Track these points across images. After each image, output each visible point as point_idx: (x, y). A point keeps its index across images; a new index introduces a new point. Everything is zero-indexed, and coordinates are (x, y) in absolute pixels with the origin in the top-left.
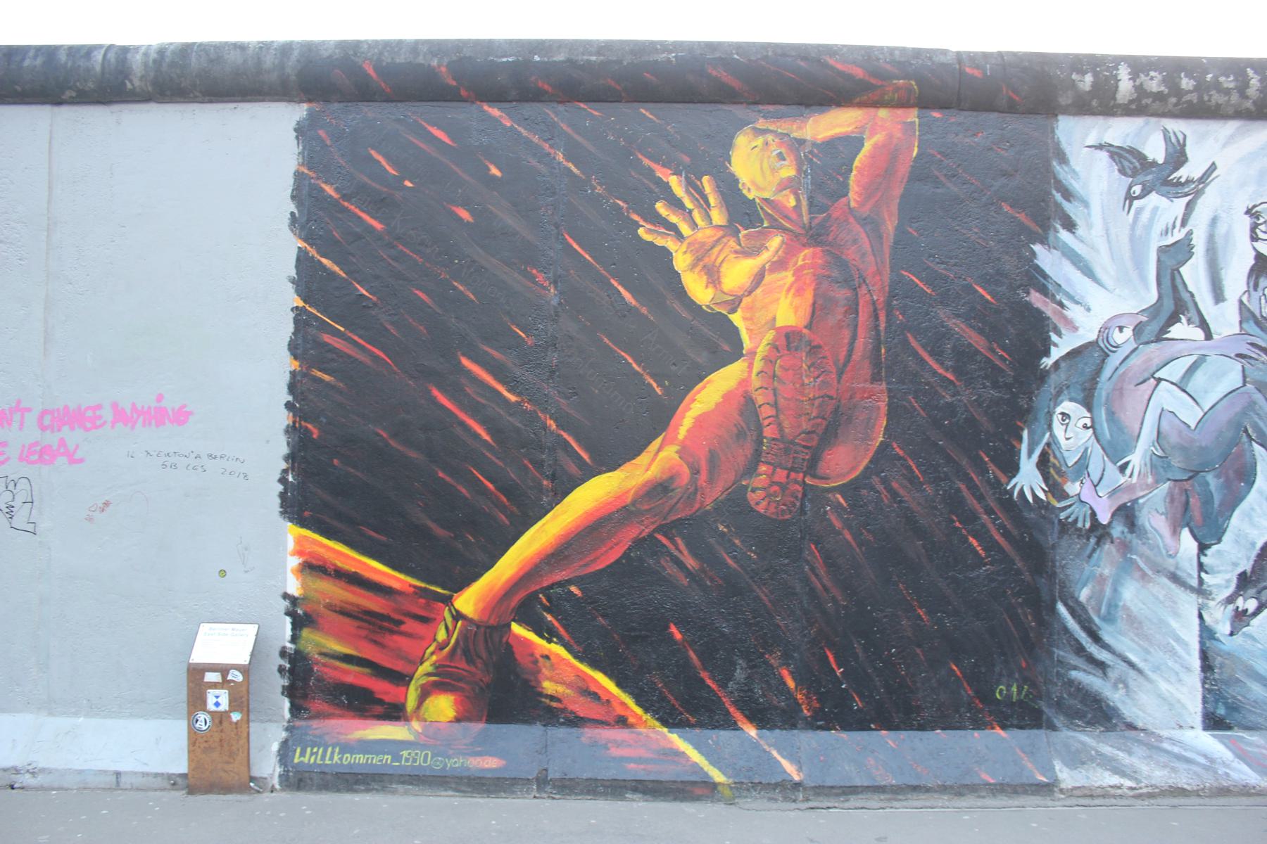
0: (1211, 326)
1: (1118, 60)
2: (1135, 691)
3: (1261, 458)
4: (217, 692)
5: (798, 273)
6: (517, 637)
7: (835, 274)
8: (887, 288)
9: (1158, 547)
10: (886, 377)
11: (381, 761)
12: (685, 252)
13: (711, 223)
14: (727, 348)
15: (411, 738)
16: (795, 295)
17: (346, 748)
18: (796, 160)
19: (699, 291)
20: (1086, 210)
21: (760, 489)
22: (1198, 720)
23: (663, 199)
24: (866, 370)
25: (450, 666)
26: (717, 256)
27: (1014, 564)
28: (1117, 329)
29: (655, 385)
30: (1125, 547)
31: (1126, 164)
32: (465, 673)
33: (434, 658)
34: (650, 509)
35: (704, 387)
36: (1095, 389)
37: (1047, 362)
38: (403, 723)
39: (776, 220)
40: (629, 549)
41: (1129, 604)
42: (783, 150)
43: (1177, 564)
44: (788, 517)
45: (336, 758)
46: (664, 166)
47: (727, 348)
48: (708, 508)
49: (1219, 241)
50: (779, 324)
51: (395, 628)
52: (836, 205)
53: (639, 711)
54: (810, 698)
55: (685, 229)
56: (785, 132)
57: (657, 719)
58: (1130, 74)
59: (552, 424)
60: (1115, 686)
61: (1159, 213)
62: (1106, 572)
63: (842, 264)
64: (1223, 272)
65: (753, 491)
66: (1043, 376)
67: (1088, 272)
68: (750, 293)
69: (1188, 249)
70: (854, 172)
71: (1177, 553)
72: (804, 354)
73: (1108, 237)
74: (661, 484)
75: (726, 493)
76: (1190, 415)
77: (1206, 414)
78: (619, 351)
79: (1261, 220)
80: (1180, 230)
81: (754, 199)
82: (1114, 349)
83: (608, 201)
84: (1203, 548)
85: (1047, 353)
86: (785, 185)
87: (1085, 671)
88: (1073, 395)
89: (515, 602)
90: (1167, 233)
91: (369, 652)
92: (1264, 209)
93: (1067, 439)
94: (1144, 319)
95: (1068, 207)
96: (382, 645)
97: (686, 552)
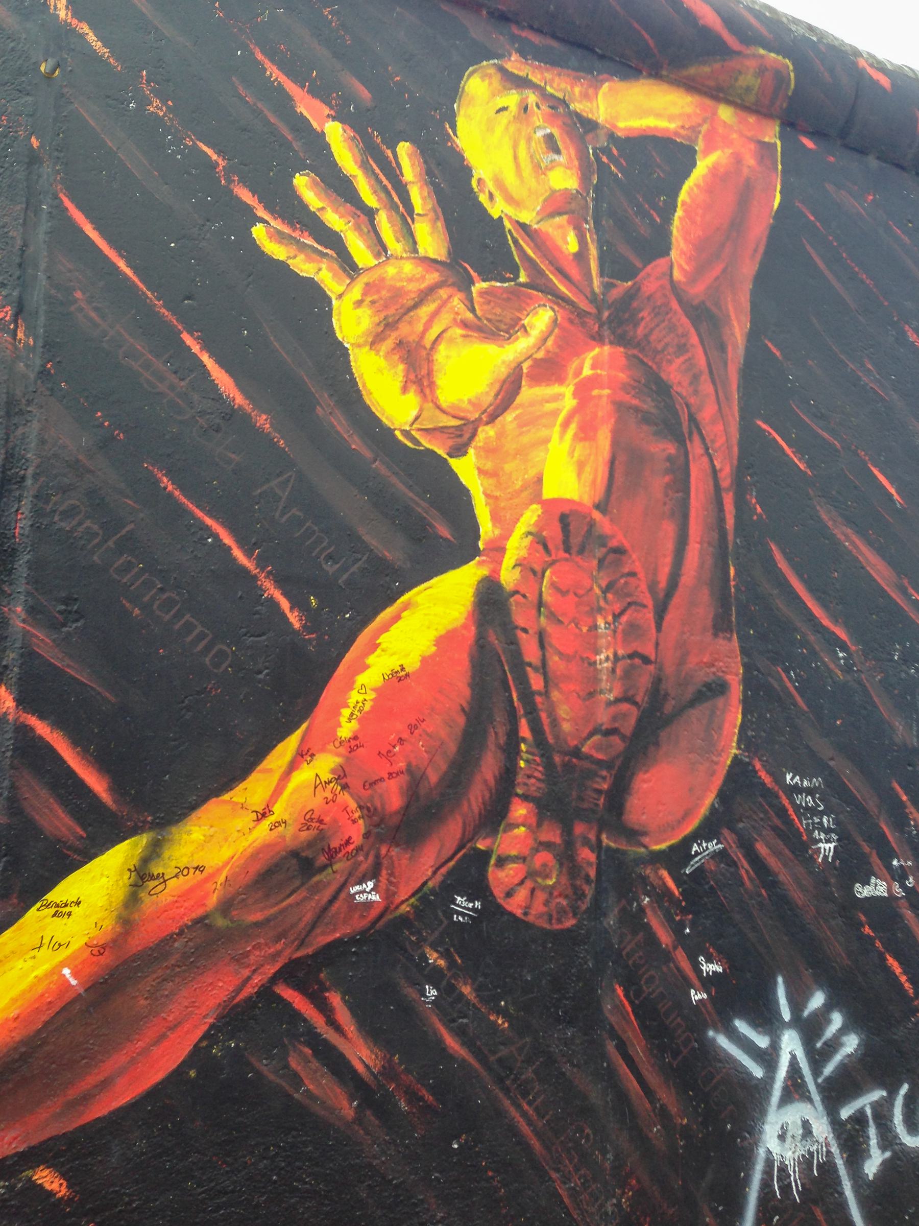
5: (583, 390)
7: (648, 405)
8: (736, 450)
10: (738, 623)
12: (359, 304)
13: (416, 251)
14: (444, 531)
16: (576, 438)
21: (514, 859)
29: (285, 604)
34: (268, 920)
35: (397, 618)
39: (541, 273)
40: (204, 1037)
42: (556, 132)
44: (570, 923)
47: (444, 531)
48: (405, 908)
50: (549, 492)
52: (649, 269)
56: (560, 95)
65: (501, 862)
68: (493, 418)
72: (595, 562)
74: (294, 854)
75: (444, 870)
78: (199, 513)
81: (500, 218)
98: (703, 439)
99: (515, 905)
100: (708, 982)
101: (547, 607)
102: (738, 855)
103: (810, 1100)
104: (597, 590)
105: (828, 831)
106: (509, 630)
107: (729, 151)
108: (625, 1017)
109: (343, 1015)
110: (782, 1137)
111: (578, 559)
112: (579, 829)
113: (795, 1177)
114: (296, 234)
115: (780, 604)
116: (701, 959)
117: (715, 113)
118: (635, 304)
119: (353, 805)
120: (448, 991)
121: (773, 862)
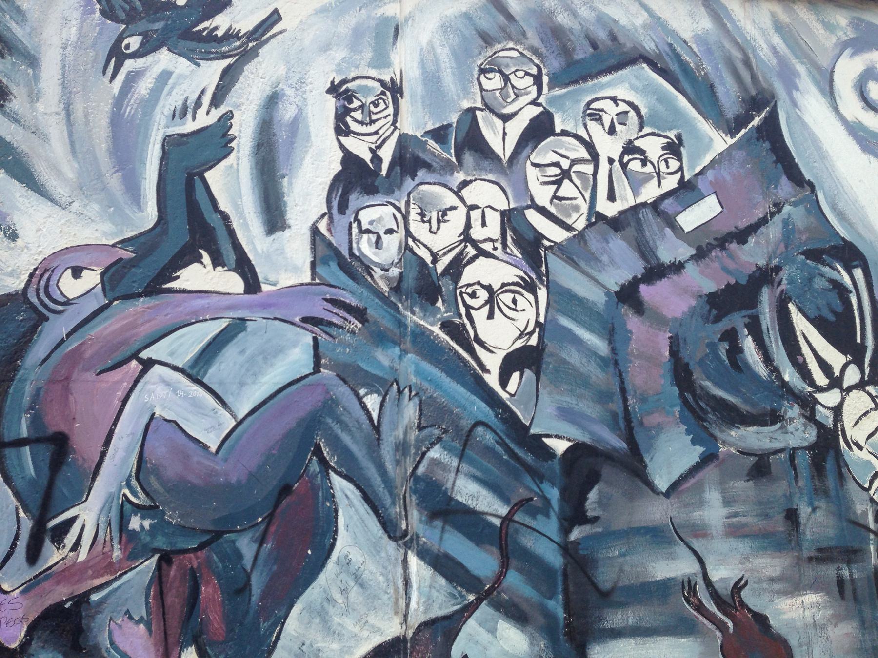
0: (258, 270)
3: (346, 501)
20: (30, 71)
28: (69, 271)
36: (12, 380)
49: (281, 135)
61: (171, 82)
64: (285, 181)
69: (224, 141)
77: (239, 424)
79: (356, 104)
80: (208, 113)
82: (61, 308)
90: (184, 114)
92: (360, 87)
94: (127, 254)
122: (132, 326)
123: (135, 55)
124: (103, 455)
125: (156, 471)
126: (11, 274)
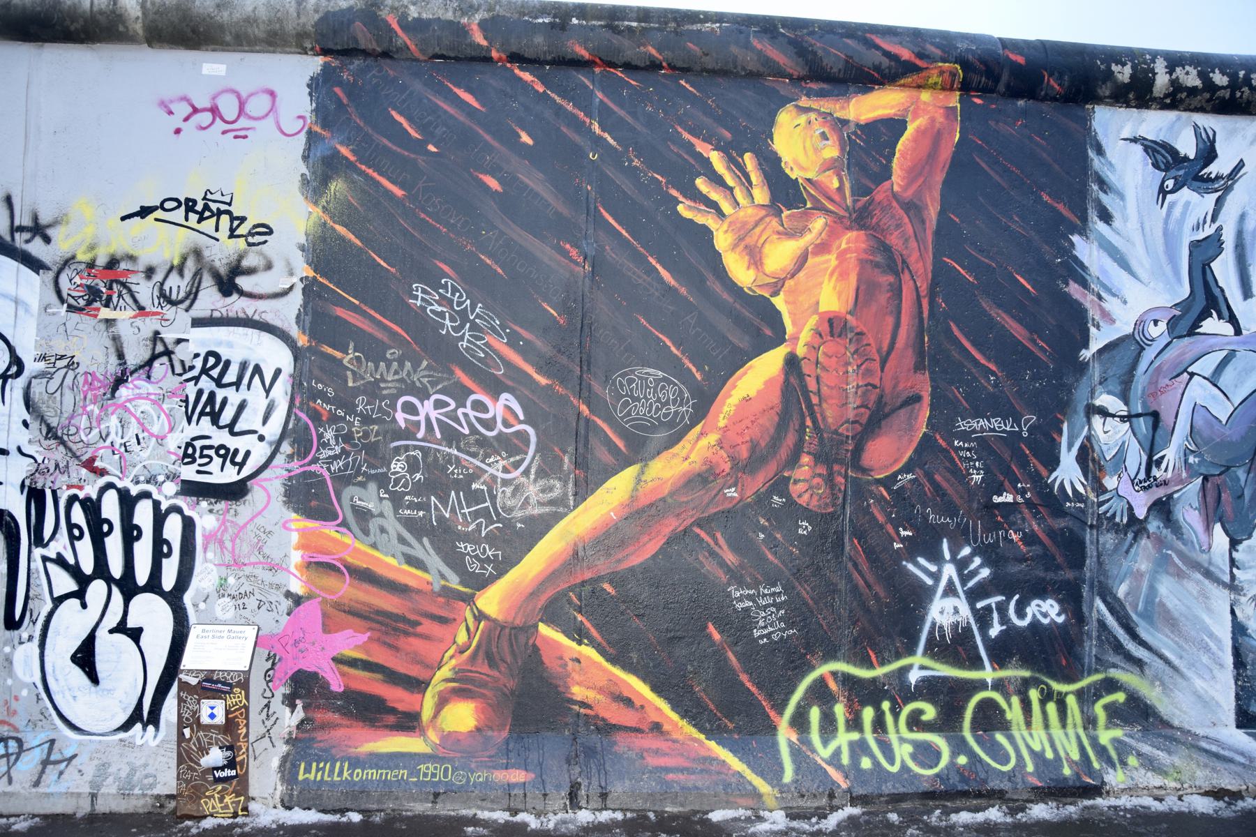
1: (1155, 54)
2: (1171, 690)
4: (212, 702)
5: (841, 256)
6: (547, 640)
7: (879, 259)
8: (930, 275)
9: (1192, 542)
11: (395, 776)
12: (726, 232)
15: (428, 750)
16: (837, 280)
17: (356, 763)
18: (840, 141)
19: (740, 272)
21: (803, 481)
22: (1230, 715)
23: (704, 175)
24: (909, 359)
25: (471, 671)
26: (760, 236)
27: (1055, 560)
29: (694, 370)
30: (1160, 542)
31: (1159, 157)
32: (488, 679)
33: (453, 662)
35: (745, 373)
37: (1086, 354)
38: (418, 733)
39: (819, 201)
41: (1164, 600)
42: (826, 130)
43: (1210, 558)
44: (831, 510)
45: (346, 774)
46: (705, 140)
47: (768, 332)
48: (749, 500)
50: (822, 308)
51: (411, 630)
52: (879, 188)
53: (674, 716)
54: (852, 700)
55: (726, 207)
56: (828, 111)
57: (694, 726)
58: (1166, 67)
59: (584, 409)
60: (1152, 683)
62: (1143, 567)
63: (886, 249)
64: (1251, 268)
65: (796, 482)
66: (1083, 367)
67: (1124, 264)
68: (793, 276)
70: (897, 155)
71: (1210, 548)
73: (1143, 230)
74: (699, 475)
76: (1222, 411)
77: (1235, 409)
83: (646, 175)
84: (1234, 544)
85: (1086, 345)
86: (829, 166)
87: (1123, 668)
88: (1111, 387)
89: (543, 599)
91: (381, 656)
93: (1105, 432)
94: (1178, 313)
95: (1106, 199)
96: (395, 648)
97: (725, 547)
98: (910, 271)
99: (803, 501)
100: (903, 540)
101: (821, 364)
102: (924, 480)
103: (959, 597)
104: (848, 354)
105: (978, 469)
106: (801, 376)
107: (926, 117)
108: (858, 552)
109: (722, 541)
110: (942, 613)
111: (838, 340)
112: (836, 467)
113: (948, 631)
114: (697, 205)
115: (955, 354)
116: (901, 529)
117: (918, 98)
118: (871, 208)
119: (725, 455)
120: (770, 536)
121: (944, 484)
122: (1183, 354)
123: (1172, 192)
124: (1175, 423)
125: (1199, 433)
126: (1126, 324)
